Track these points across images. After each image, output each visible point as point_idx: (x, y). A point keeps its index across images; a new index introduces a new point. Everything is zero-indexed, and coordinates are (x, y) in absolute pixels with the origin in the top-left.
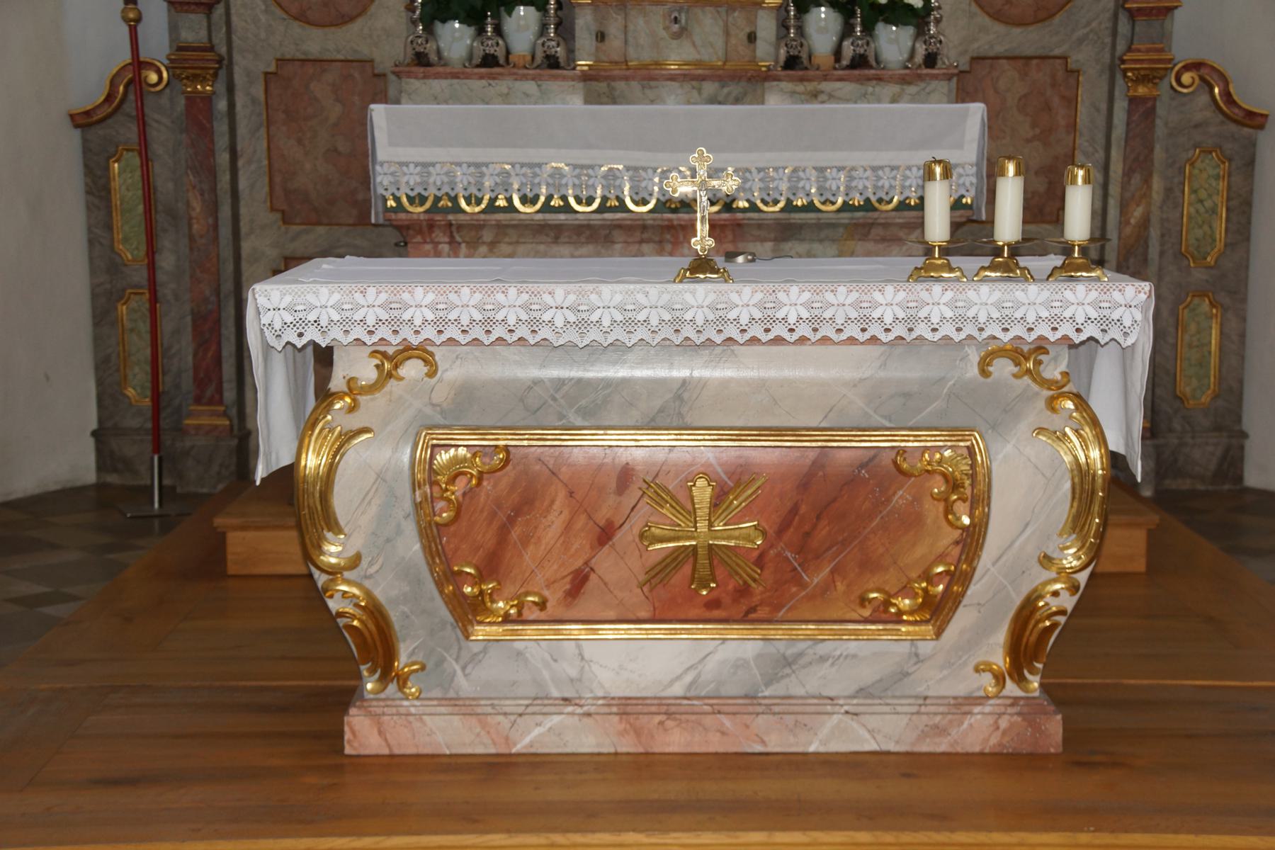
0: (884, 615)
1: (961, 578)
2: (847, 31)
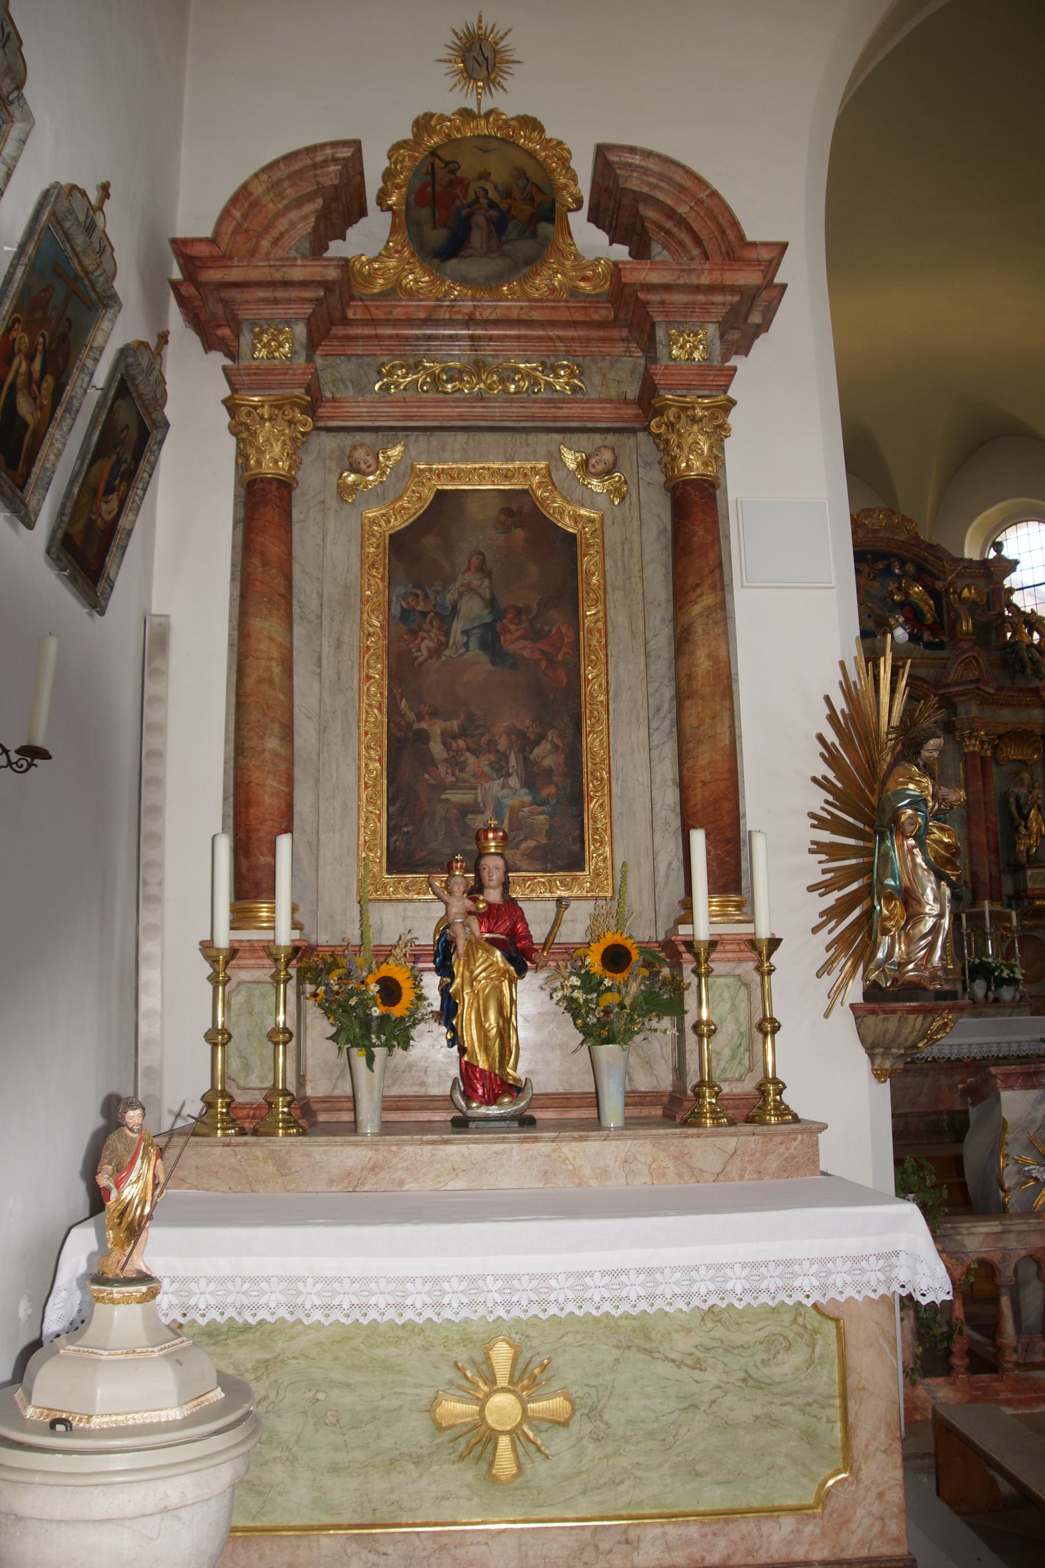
2: (989, 989)
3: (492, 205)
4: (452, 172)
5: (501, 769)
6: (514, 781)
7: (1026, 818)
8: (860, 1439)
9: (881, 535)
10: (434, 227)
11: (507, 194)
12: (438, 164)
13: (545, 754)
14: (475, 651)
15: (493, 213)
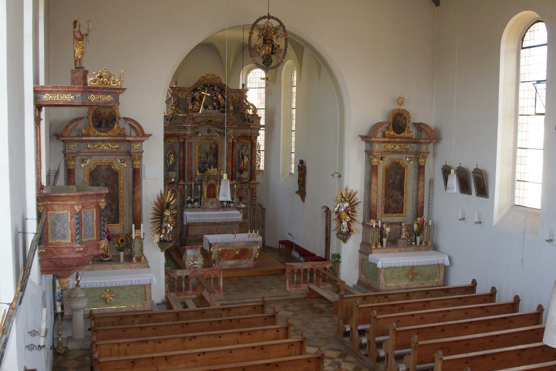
0: (246, 258)
1: (251, 256)
2: (227, 203)
3: (106, 118)
4: (99, 112)
6: (109, 211)
7: (243, 158)
8: (147, 298)
9: (211, 81)
10: (96, 122)
11: (108, 116)
12: (97, 111)
15: (106, 120)
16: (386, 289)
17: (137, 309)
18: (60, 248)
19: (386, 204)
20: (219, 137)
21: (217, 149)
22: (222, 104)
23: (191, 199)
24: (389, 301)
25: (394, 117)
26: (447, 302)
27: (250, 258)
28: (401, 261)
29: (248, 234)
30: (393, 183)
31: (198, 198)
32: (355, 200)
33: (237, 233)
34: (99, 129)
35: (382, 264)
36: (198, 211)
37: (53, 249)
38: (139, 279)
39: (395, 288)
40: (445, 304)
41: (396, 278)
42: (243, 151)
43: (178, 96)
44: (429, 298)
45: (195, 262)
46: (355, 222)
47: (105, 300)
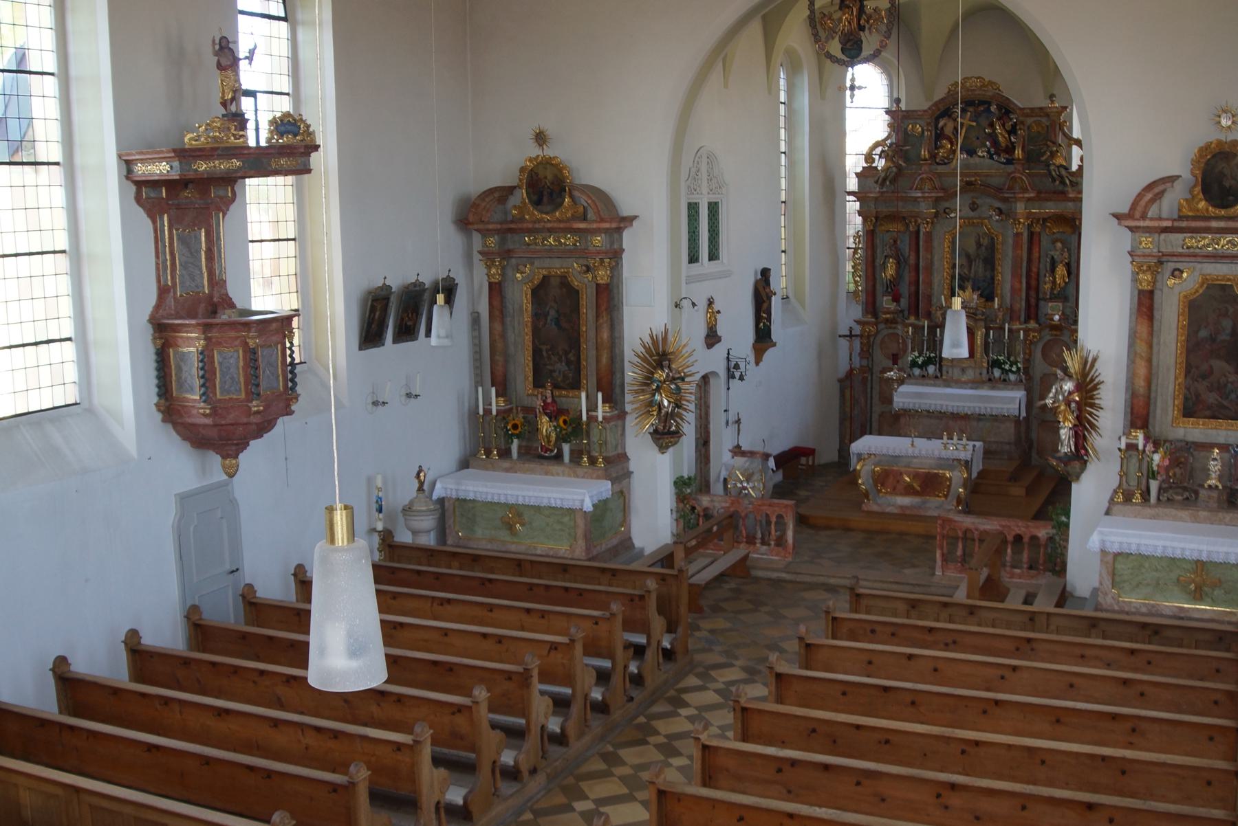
0: (938, 496)
1: (948, 492)
2: (1003, 373)
3: (549, 187)
5: (560, 360)
6: (564, 364)
7: (1053, 270)
9: (977, 92)
13: (571, 357)
14: (554, 326)
15: (549, 190)
16: (1116, 608)
17: (561, 553)
18: (186, 406)
19: (1190, 393)
20: (997, 221)
21: (992, 247)
22: (1003, 145)
23: (919, 357)
24: (979, 625)
25: (1207, 163)
26: (1088, 652)
27: (946, 496)
28: (1161, 543)
29: (941, 441)
30: (1212, 339)
31: (935, 357)
32: (1093, 376)
33: (915, 437)
34: (539, 207)
35: (1103, 542)
36: (935, 385)
37: (179, 408)
38: (560, 496)
39: (1144, 610)
40: (1083, 656)
41: (1148, 585)
42: (1056, 255)
43: (906, 129)
44: (1097, 637)
45: (745, 485)
46: (1093, 432)
47: (510, 527)
